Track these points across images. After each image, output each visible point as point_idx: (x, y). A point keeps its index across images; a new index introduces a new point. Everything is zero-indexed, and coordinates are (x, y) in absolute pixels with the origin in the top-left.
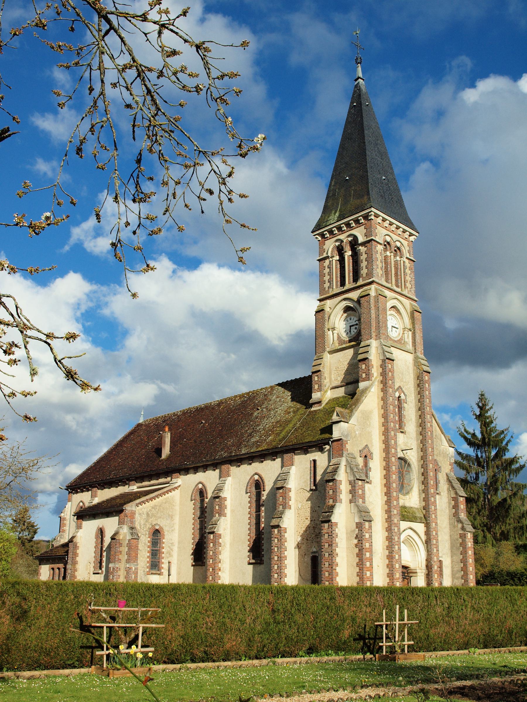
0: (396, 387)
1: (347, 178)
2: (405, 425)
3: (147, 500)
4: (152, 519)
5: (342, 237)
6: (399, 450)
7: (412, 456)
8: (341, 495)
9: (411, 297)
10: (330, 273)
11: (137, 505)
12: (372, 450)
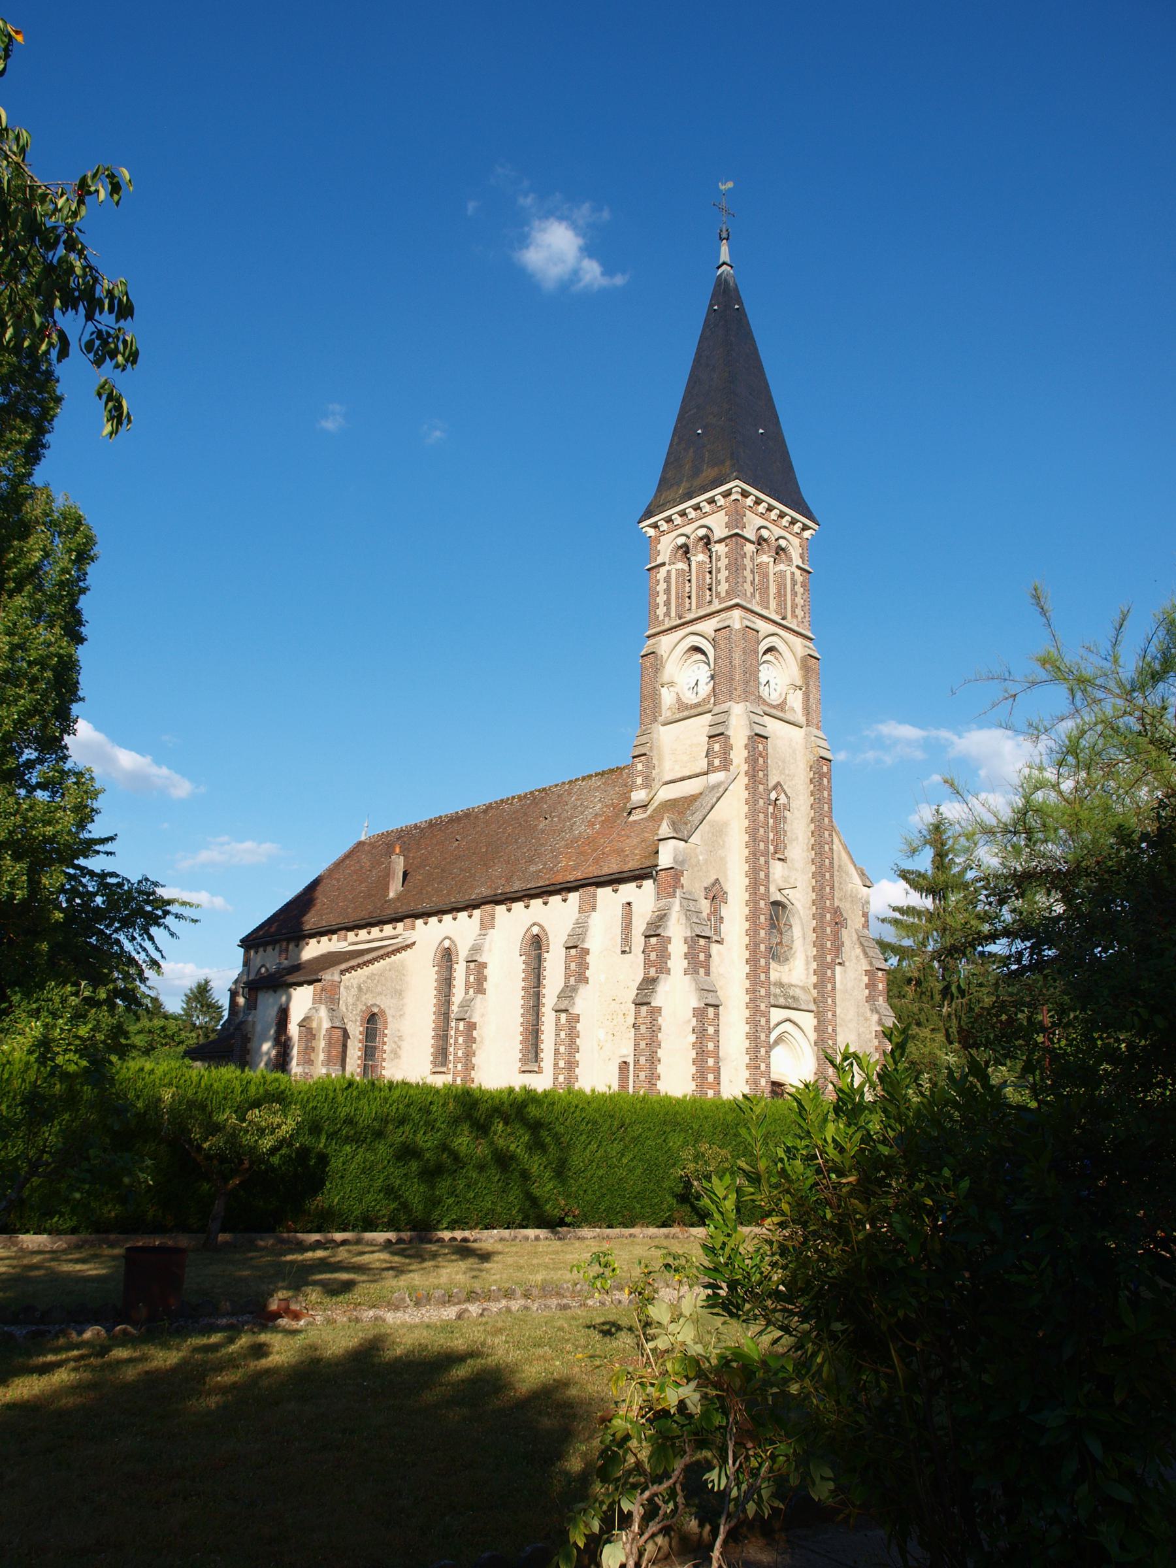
0: (771, 784)
1: (699, 431)
2: (785, 848)
3: (359, 966)
4: (367, 996)
5: (687, 530)
6: (772, 889)
7: (796, 899)
8: (669, 961)
10: (668, 591)
11: (342, 973)
12: (726, 889)
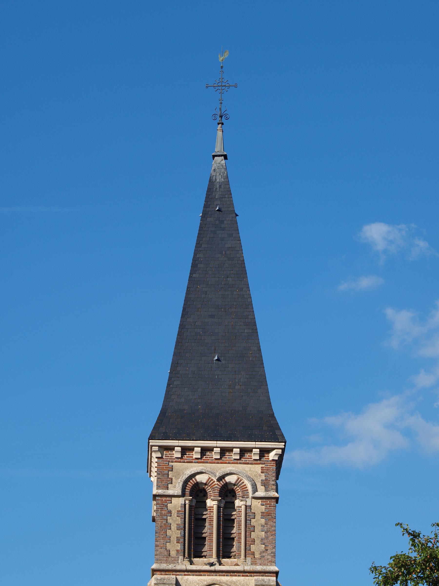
9: (259, 568)
